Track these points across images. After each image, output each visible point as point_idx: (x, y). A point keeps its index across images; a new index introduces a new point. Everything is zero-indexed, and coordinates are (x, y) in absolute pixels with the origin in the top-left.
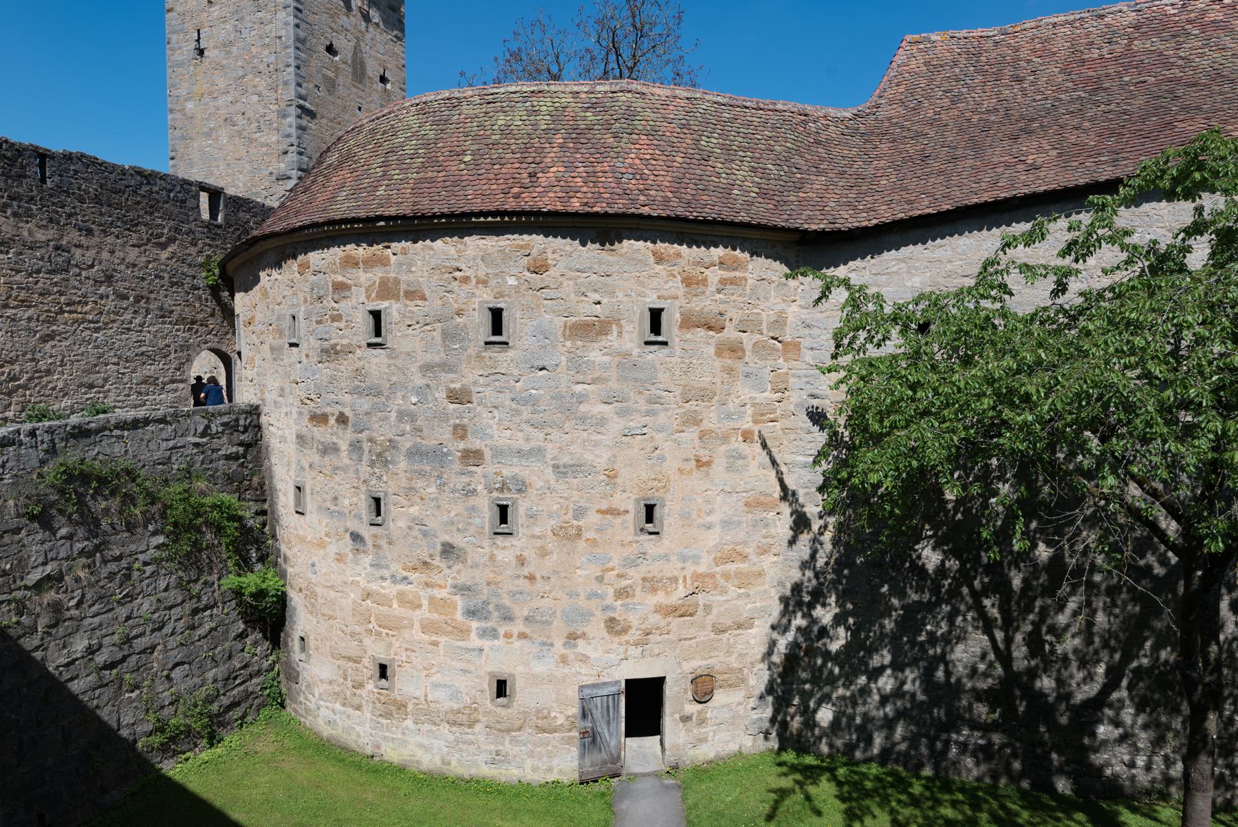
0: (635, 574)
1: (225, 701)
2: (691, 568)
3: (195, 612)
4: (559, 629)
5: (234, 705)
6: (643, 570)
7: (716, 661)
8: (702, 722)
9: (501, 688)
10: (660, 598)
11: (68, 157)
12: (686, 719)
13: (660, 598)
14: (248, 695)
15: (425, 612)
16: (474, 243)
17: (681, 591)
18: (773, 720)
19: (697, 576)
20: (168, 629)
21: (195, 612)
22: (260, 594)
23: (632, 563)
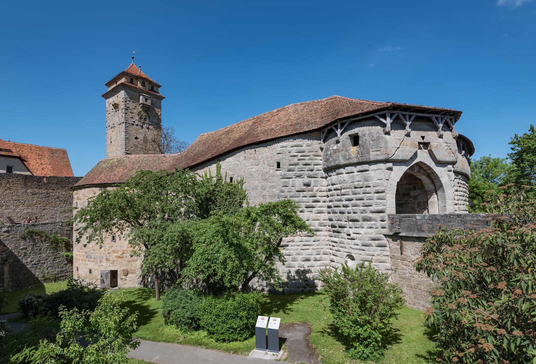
0: (111, 250)
1: (60, 275)
2: (122, 249)
3: (55, 258)
4: (98, 260)
5: (61, 277)
6: (113, 249)
7: (129, 268)
8: (126, 280)
9: (90, 271)
10: (116, 254)
11: (50, 177)
12: (122, 279)
13: (116, 254)
14: (66, 276)
15: (81, 258)
16: (87, 190)
17: (120, 253)
18: (142, 281)
19: (123, 250)
20: (48, 260)
21: (55, 258)
22: (67, 256)
23: (110, 247)
